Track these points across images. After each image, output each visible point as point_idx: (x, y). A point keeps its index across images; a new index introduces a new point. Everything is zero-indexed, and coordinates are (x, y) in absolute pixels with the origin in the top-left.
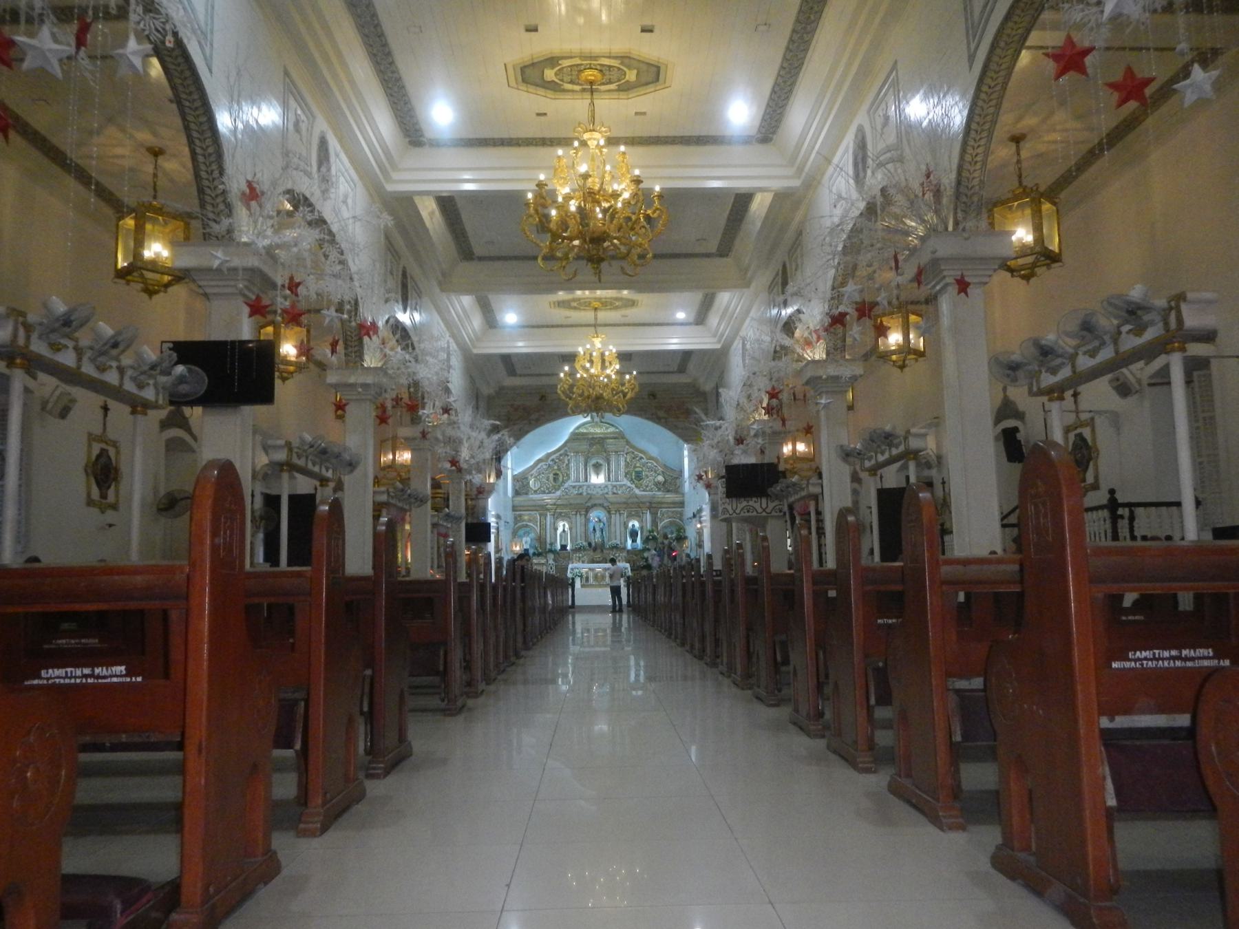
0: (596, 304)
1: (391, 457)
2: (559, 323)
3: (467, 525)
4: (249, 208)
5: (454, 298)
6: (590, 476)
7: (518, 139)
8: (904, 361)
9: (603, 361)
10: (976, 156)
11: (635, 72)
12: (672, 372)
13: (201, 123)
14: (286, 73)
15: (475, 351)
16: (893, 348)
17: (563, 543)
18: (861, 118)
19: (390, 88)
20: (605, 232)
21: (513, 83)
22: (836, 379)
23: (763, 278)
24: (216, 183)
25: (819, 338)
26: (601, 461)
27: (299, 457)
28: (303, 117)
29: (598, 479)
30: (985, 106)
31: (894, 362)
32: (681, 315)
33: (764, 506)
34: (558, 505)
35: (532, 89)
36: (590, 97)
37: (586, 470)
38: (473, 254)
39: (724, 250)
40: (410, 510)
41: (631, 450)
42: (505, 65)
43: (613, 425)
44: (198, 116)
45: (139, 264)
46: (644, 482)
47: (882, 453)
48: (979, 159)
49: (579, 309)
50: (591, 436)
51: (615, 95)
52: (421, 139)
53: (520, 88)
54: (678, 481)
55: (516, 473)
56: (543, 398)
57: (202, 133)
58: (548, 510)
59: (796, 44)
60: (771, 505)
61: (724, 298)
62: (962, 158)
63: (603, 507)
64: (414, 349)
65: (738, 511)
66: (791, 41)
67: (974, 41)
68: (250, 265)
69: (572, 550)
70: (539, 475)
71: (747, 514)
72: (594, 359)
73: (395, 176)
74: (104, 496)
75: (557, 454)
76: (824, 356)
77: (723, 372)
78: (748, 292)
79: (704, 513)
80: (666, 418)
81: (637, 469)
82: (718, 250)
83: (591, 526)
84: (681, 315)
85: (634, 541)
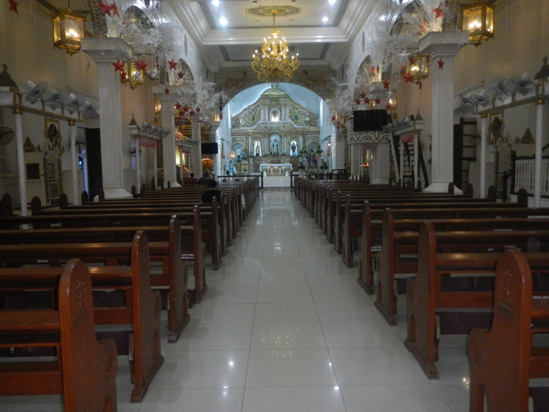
0: (274, 11)
2: (252, 25)
3: (202, 145)
6: (271, 117)
9: (279, 48)
12: (317, 59)
15: (204, 43)
17: (257, 152)
26: (277, 110)
29: (275, 119)
34: (254, 133)
41: (292, 104)
43: (282, 90)
46: (299, 121)
50: (271, 97)
54: (317, 121)
55: (233, 116)
56: (245, 74)
58: (249, 135)
60: (381, 136)
63: (279, 134)
65: (360, 139)
69: (262, 156)
71: (366, 141)
72: (272, 46)
75: (254, 106)
77: (347, 57)
79: (332, 138)
80: (312, 85)
83: (272, 143)
85: (294, 151)
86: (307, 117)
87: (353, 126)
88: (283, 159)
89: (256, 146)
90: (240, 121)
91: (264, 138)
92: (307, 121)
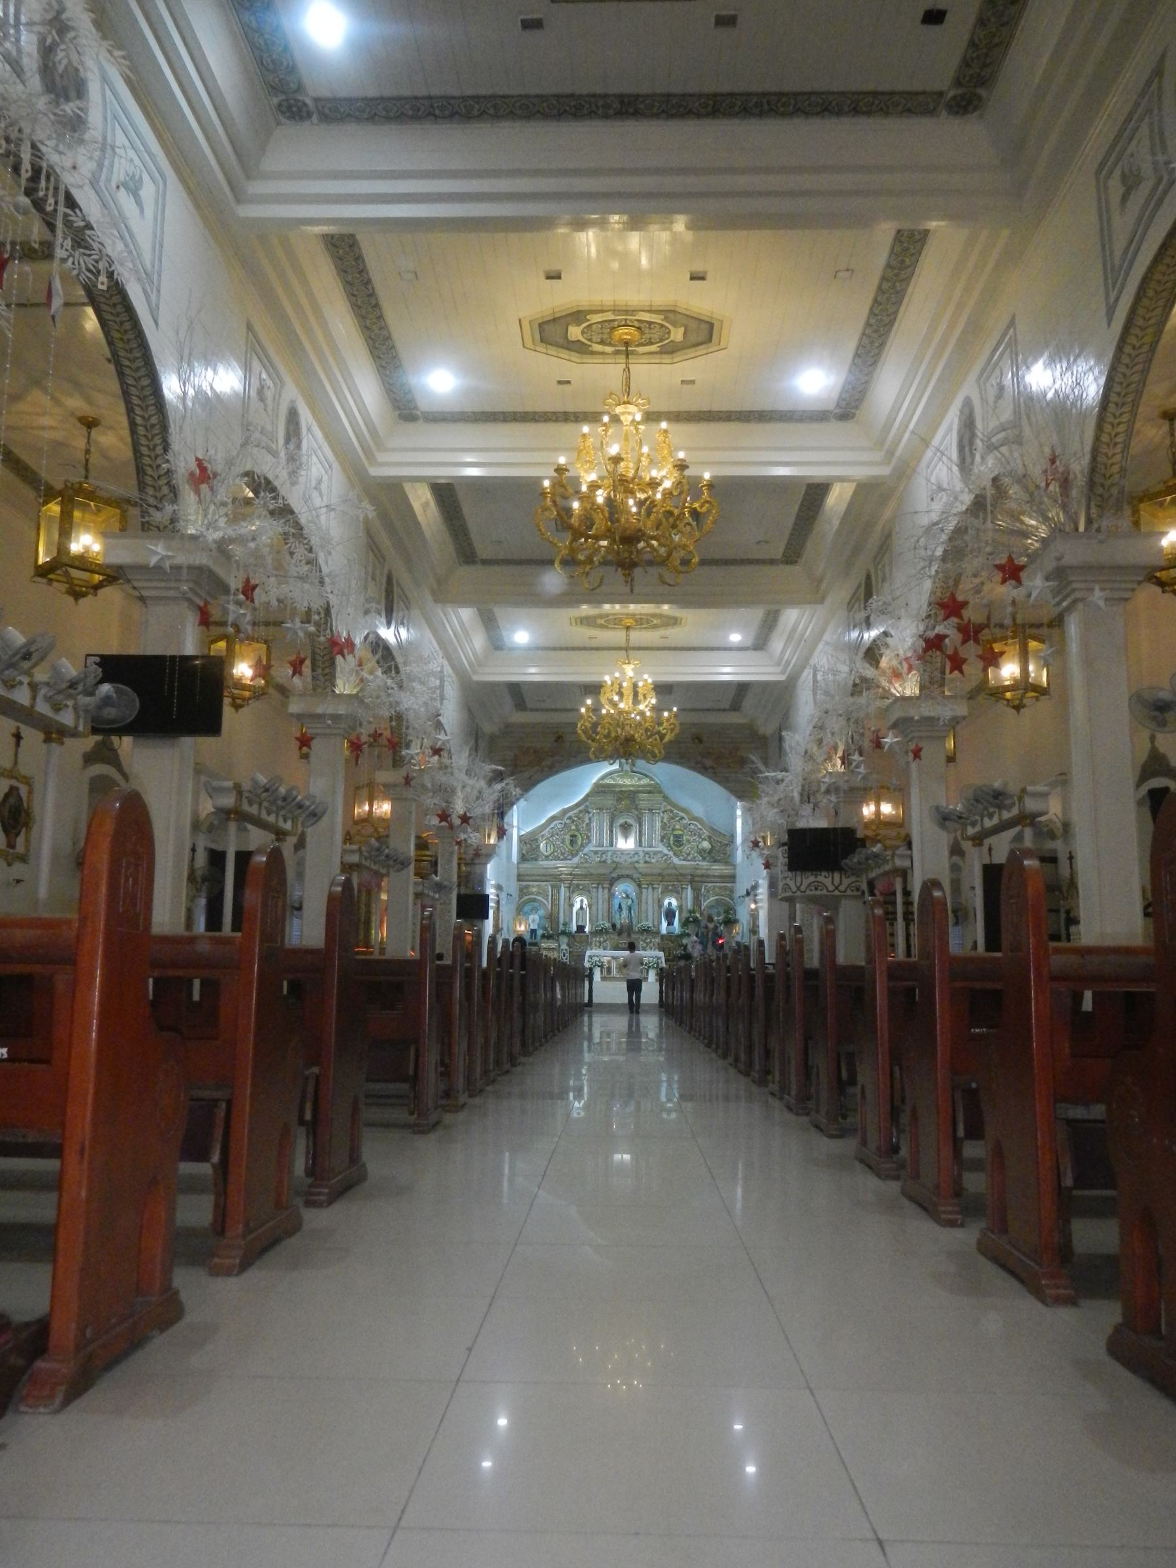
0: (629, 622)
1: (367, 808)
3: (459, 897)
4: (197, 492)
5: (450, 610)
6: (617, 839)
7: (535, 413)
8: (1021, 700)
9: (636, 694)
10: (1115, 436)
11: (681, 330)
13: (143, 388)
14: (250, 328)
15: (476, 678)
16: (1007, 683)
17: (580, 923)
18: (969, 389)
19: (377, 348)
20: (640, 530)
21: (529, 343)
22: (930, 721)
23: (840, 593)
24: (159, 461)
25: (910, 669)
26: (630, 821)
27: (251, 803)
28: (269, 383)
29: (626, 844)
30: (1128, 374)
31: (1008, 700)
32: (735, 638)
33: (837, 882)
34: (575, 875)
35: (552, 350)
36: (624, 361)
37: (611, 831)
38: (476, 556)
39: (792, 556)
40: (388, 875)
41: (669, 807)
42: (520, 320)
43: (646, 776)
44: (140, 378)
45: (65, 560)
46: (686, 849)
47: (991, 816)
48: (1119, 440)
49: (606, 627)
51: (657, 359)
52: (414, 412)
53: (538, 349)
54: (728, 849)
55: (523, 833)
56: (559, 739)
57: (143, 399)
58: (561, 880)
59: (886, 296)
60: (846, 882)
61: (791, 616)
62: (1097, 439)
64: (398, 671)
65: (803, 888)
66: (880, 288)
67: (1114, 286)
68: (197, 563)
69: (591, 933)
70: (552, 836)
71: (814, 892)
72: (623, 690)
73: (381, 457)
74: (11, 845)
76: (918, 692)
78: (821, 611)
79: (760, 891)
81: (676, 833)
82: (784, 555)
83: (616, 903)
84: (735, 638)
85: (670, 923)
86: (704, 839)
87: (787, 860)
88: (644, 941)
89: (577, 906)
90: (538, 846)
91: (597, 888)
92: (705, 851)
